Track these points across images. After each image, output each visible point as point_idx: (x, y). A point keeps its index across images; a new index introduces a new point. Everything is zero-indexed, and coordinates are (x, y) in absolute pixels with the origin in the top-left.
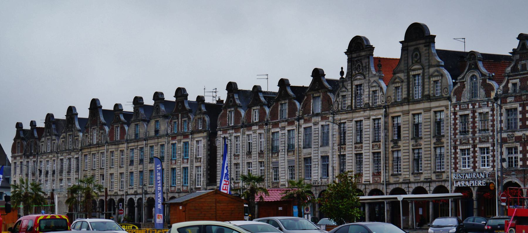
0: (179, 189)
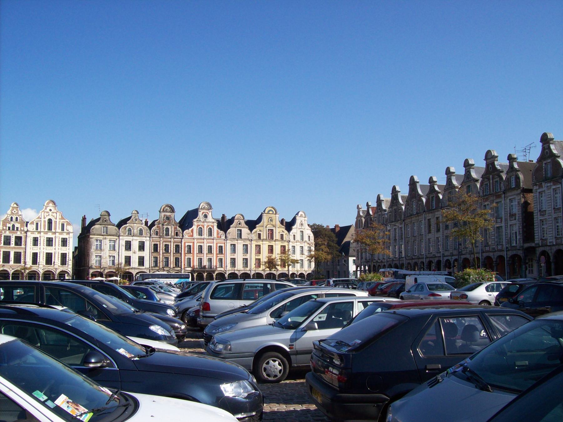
0: (494, 249)
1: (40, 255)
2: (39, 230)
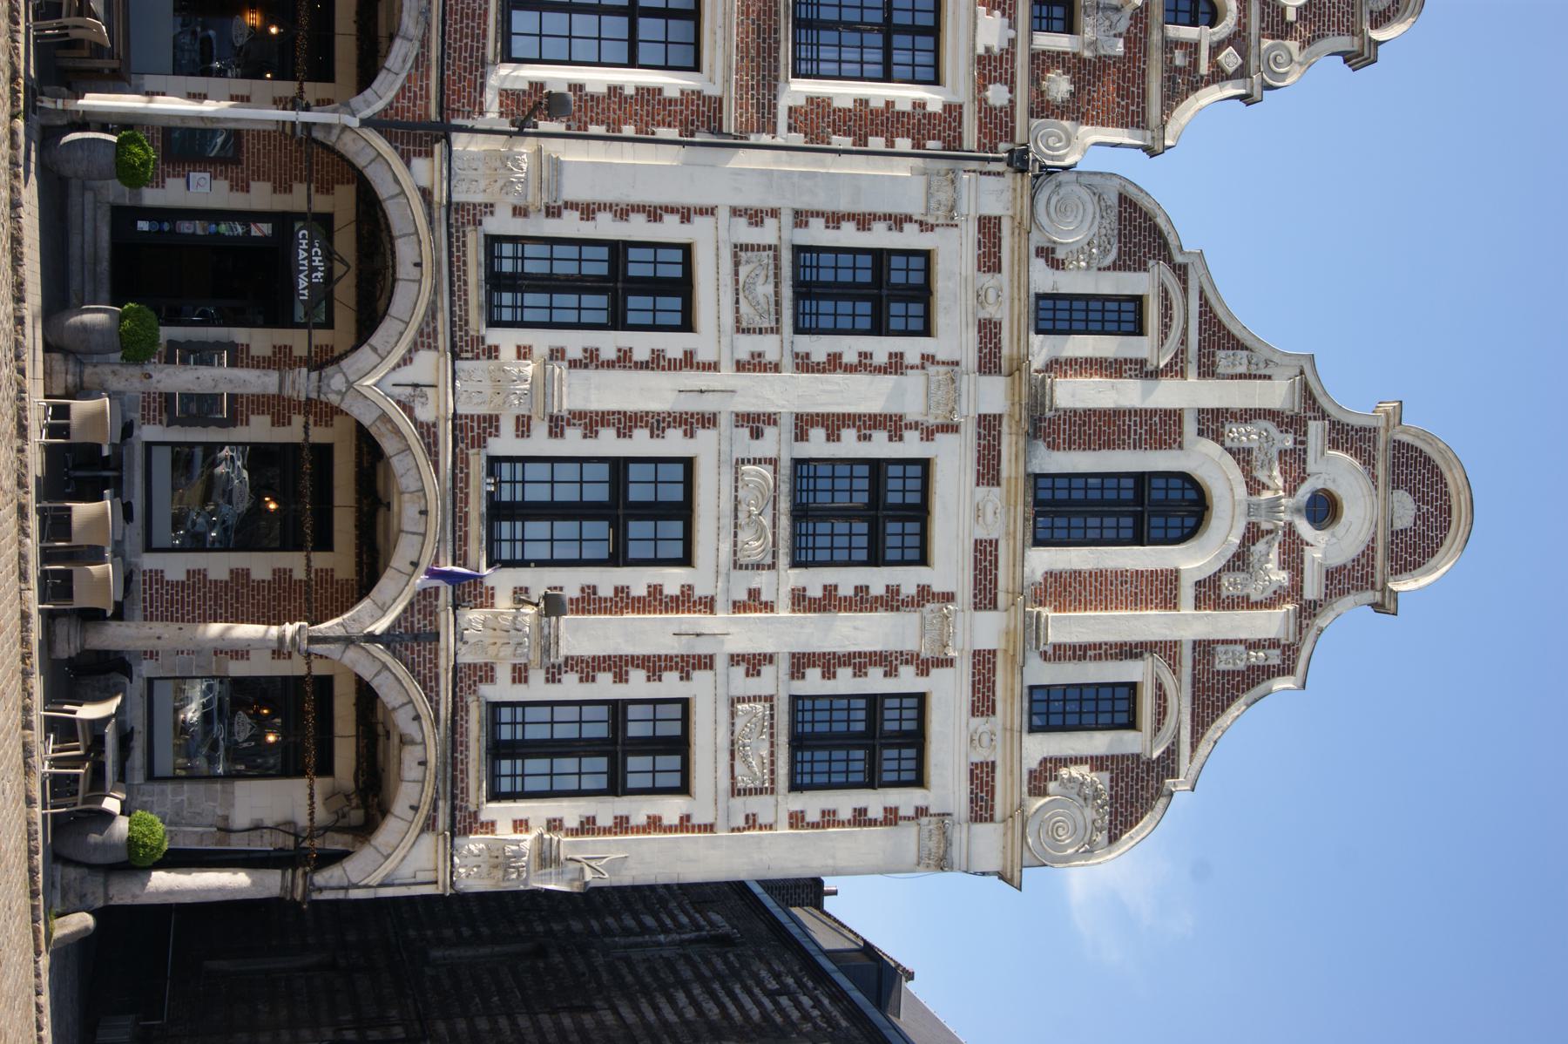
1: (657, 362)
2: (1042, 348)
